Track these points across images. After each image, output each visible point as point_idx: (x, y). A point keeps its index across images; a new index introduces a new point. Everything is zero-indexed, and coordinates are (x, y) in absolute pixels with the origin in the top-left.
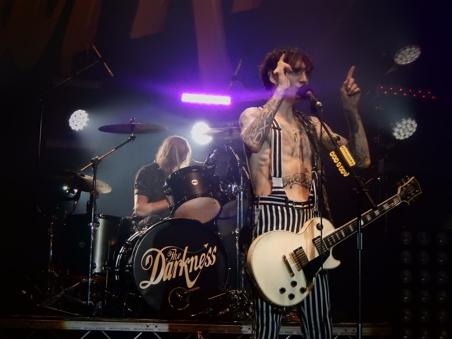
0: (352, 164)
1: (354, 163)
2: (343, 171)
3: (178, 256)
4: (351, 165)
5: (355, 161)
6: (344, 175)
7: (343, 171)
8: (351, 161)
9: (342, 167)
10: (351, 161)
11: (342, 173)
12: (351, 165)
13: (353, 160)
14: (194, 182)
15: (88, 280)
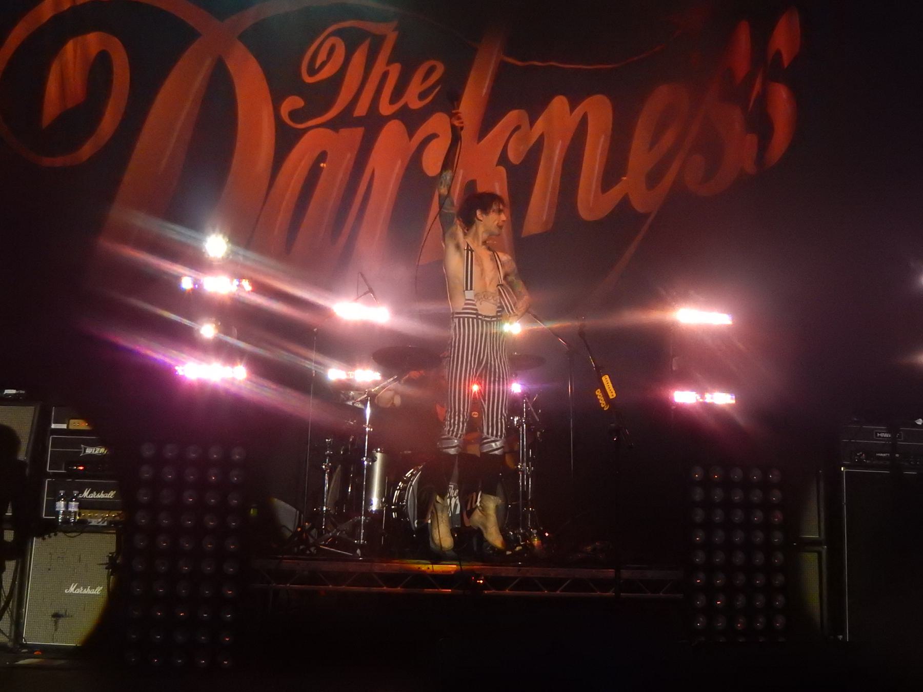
0: (613, 395)
1: (615, 395)
2: (603, 404)
3: (455, 493)
4: (611, 397)
5: (616, 392)
6: (605, 409)
7: (603, 404)
8: (612, 392)
9: (602, 398)
10: (612, 392)
11: (602, 406)
12: (611, 397)
13: (614, 392)
14: (474, 414)
15: (361, 518)
